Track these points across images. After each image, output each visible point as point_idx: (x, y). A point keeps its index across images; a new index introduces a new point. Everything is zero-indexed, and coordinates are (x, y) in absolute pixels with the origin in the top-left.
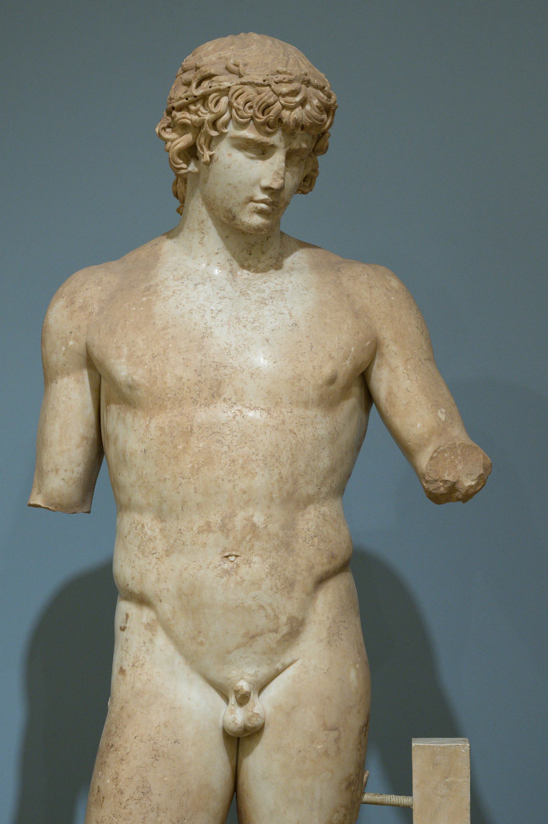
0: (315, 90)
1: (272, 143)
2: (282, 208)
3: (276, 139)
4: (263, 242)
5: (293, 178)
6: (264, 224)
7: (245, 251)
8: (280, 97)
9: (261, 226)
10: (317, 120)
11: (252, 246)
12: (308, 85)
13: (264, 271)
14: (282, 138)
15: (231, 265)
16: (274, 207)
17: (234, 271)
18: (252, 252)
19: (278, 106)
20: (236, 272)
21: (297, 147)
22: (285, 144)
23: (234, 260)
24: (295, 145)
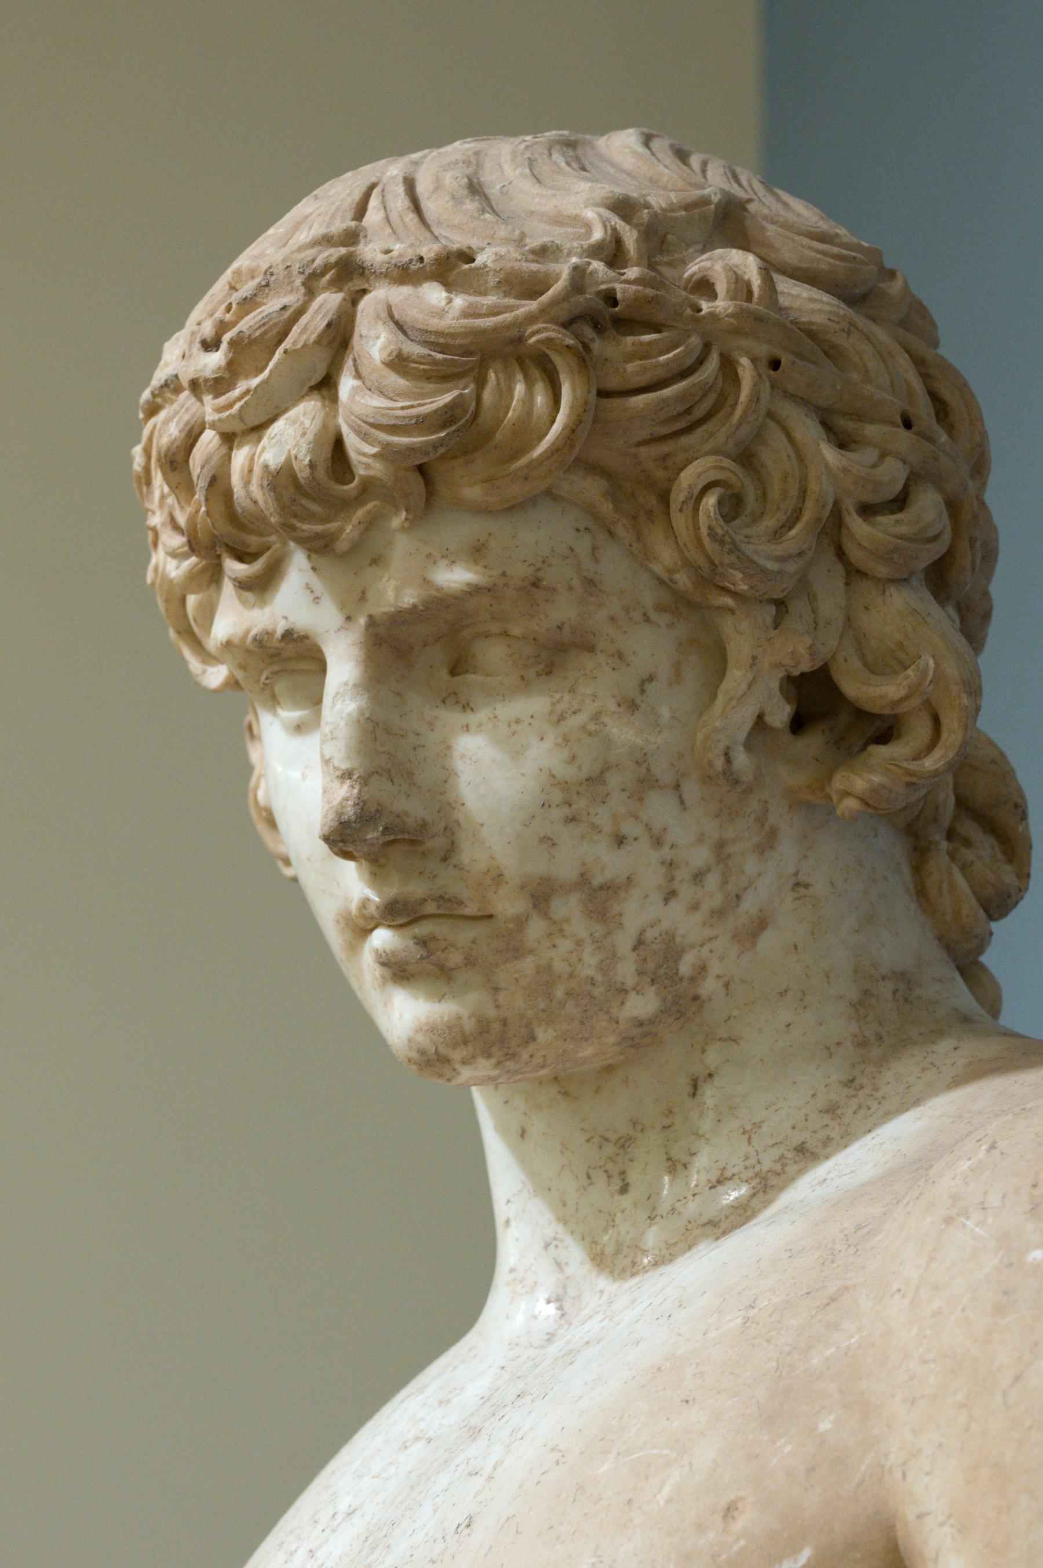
0: (397, 294)
1: (281, 628)
2: (521, 922)
3: (299, 599)
4: (671, 1112)
5: (517, 754)
6: (431, 1029)
7: (600, 1178)
8: (208, 398)
9: (420, 1038)
10: (394, 429)
11: (624, 1144)
12: (358, 284)
13: (666, 1257)
14: (315, 581)
15: (559, 1265)
16: (421, 929)
17: (572, 1292)
18: (632, 1177)
19: (209, 439)
20: (578, 1297)
21: (409, 598)
22: (342, 606)
23: (569, 1241)
24: (395, 591)
